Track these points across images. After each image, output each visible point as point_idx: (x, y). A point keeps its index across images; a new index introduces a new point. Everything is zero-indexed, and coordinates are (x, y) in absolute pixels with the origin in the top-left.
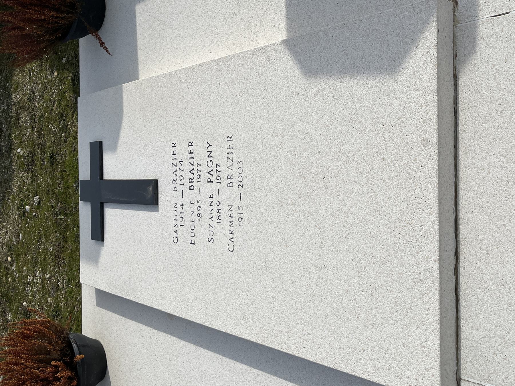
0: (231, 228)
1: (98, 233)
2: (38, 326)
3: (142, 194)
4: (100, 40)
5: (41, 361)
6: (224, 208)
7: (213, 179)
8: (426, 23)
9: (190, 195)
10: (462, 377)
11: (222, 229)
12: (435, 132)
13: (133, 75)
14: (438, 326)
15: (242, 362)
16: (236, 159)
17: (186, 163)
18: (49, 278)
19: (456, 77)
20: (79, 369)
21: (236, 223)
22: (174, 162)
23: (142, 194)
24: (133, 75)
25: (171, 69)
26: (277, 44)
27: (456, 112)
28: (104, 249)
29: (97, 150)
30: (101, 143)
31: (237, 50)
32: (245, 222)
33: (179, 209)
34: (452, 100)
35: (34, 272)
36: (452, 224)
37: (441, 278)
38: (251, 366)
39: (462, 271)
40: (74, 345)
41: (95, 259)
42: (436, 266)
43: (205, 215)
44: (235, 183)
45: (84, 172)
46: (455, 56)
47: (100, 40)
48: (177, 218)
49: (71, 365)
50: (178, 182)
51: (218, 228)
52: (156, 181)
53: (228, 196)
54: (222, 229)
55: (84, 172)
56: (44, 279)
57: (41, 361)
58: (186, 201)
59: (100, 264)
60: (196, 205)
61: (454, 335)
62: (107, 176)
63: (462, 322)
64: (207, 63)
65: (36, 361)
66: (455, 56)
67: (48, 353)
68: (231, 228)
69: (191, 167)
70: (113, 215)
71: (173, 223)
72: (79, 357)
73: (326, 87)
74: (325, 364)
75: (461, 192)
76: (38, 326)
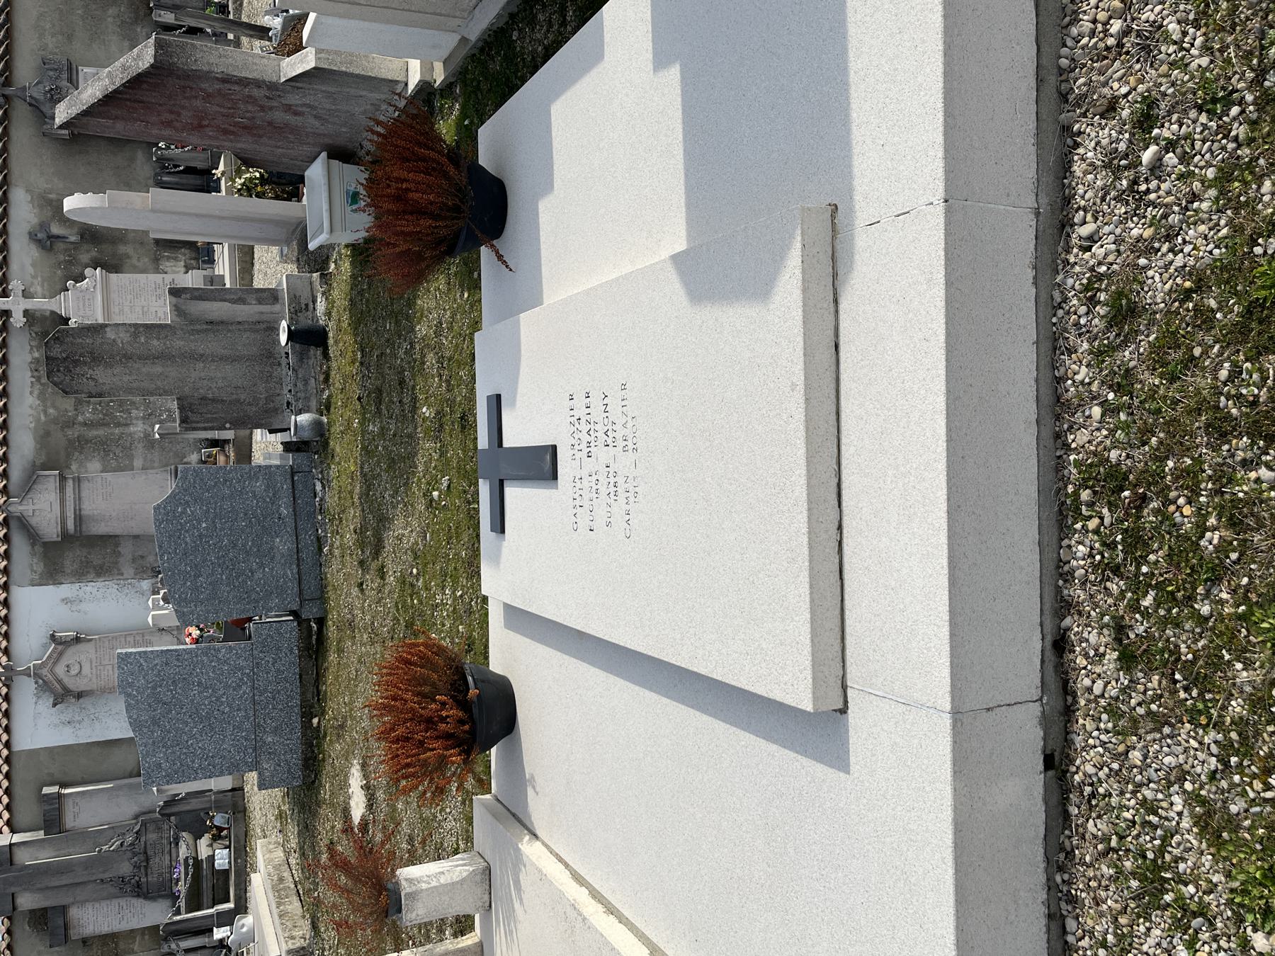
0: (628, 507)
1: (499, 526)
2: (422, 648)
3: (541, 465)
4: (497, 252)
5: (424, 696)
6: (620, 480)
7: (609, 441)
8: (792, 237)
9: (589, 465)
10: (849, 684)
11: (619, 508)
12: (802, 373)
13: (535, 300)
14: (809, 616)
15: (651, 689)
16: (630, 415)
17: (583, 421)
18: (461, 596)
19: (836, 301)
20: (475, 711)
21: (632, 499)
22: (572, 419)
23: (541, 465)
24: (536, 300)
25: (594, 282)
26: (664, 261)
27: (837, 347)
28: (505, 544)
29: (496, 403)
30: (499, 397)
31: (627, 268)
32: (640, 497)
33: (578, 485)
34: (831, 333)
35: (443, 588)
36: (835, 490)
37: (811, 556)
38: (659, 693)
39: (845, 548)
40: (470, 679)
41: (496, 559)
42: (805, 540)
43: (603, 490)
44: (631, 446)
45: (483, 442)
46: (835, 276)
47: (497, 252)
48: (576, 496)
49: (464, 704)
50: (577, 447)
51: (615, 509)
52: (554, 448)
53: (624, 463)
54: (619, 508)
55: (483, 442)
56: (455, 599)
57: (424, 696)
58: (585, 473)
59: (502, 566)
60: (594, 478)
61: (838, 629)
62: (506, 444)
63: (847, 613)
64: (601, 286)
65: (419, 694)
66: (835, 276)
67: (433, 685)
68: (628, 507)
69: (589, 426)
70: (513, 493)
71: (571, 503)
72: (473, 692)
73: (711, 314)
74: (715, 677)
75: (843, 448)
76: (422, 648)
